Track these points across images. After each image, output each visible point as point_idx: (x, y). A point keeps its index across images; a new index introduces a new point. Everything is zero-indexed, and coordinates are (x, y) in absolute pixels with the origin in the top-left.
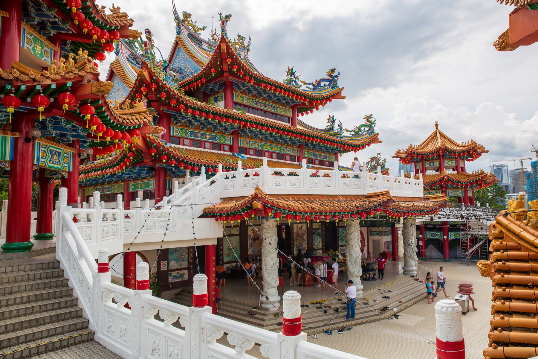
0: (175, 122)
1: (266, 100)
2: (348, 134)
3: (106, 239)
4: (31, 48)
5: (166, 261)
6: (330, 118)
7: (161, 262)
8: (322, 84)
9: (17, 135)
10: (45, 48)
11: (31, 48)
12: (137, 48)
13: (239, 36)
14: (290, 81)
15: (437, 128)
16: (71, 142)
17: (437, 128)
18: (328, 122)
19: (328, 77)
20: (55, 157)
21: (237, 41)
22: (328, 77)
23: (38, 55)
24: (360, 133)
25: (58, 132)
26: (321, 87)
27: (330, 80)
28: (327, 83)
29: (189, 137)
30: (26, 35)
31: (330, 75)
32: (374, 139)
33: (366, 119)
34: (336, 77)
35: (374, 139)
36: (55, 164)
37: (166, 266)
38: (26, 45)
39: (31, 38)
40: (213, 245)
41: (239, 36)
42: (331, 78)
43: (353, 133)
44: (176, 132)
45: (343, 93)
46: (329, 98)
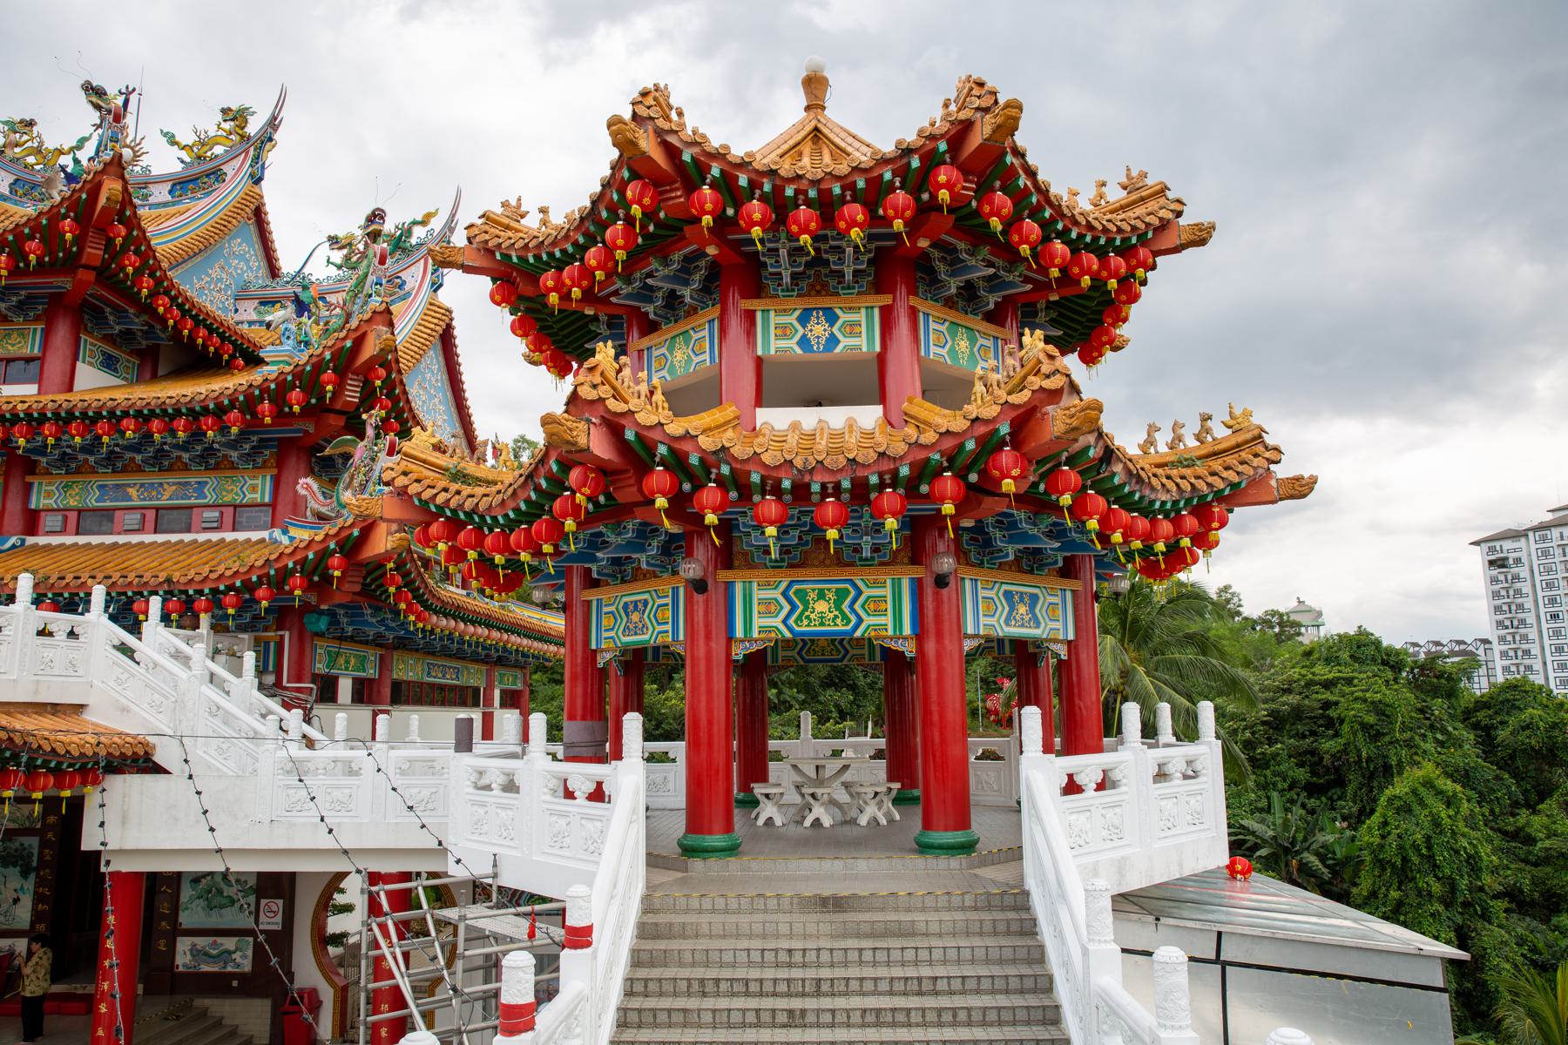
3: (1169, 833)
4: (943, 352)
9: (918, 572)
10: (981, 341)
11: (943, 352)
16: (1060, 564)
20: (1022, 609)
23: (964, 362)
25: (1021, 547)
30: (932, 325)
36: (1022, 626)
38: (933, 349)
39: (943, 328)
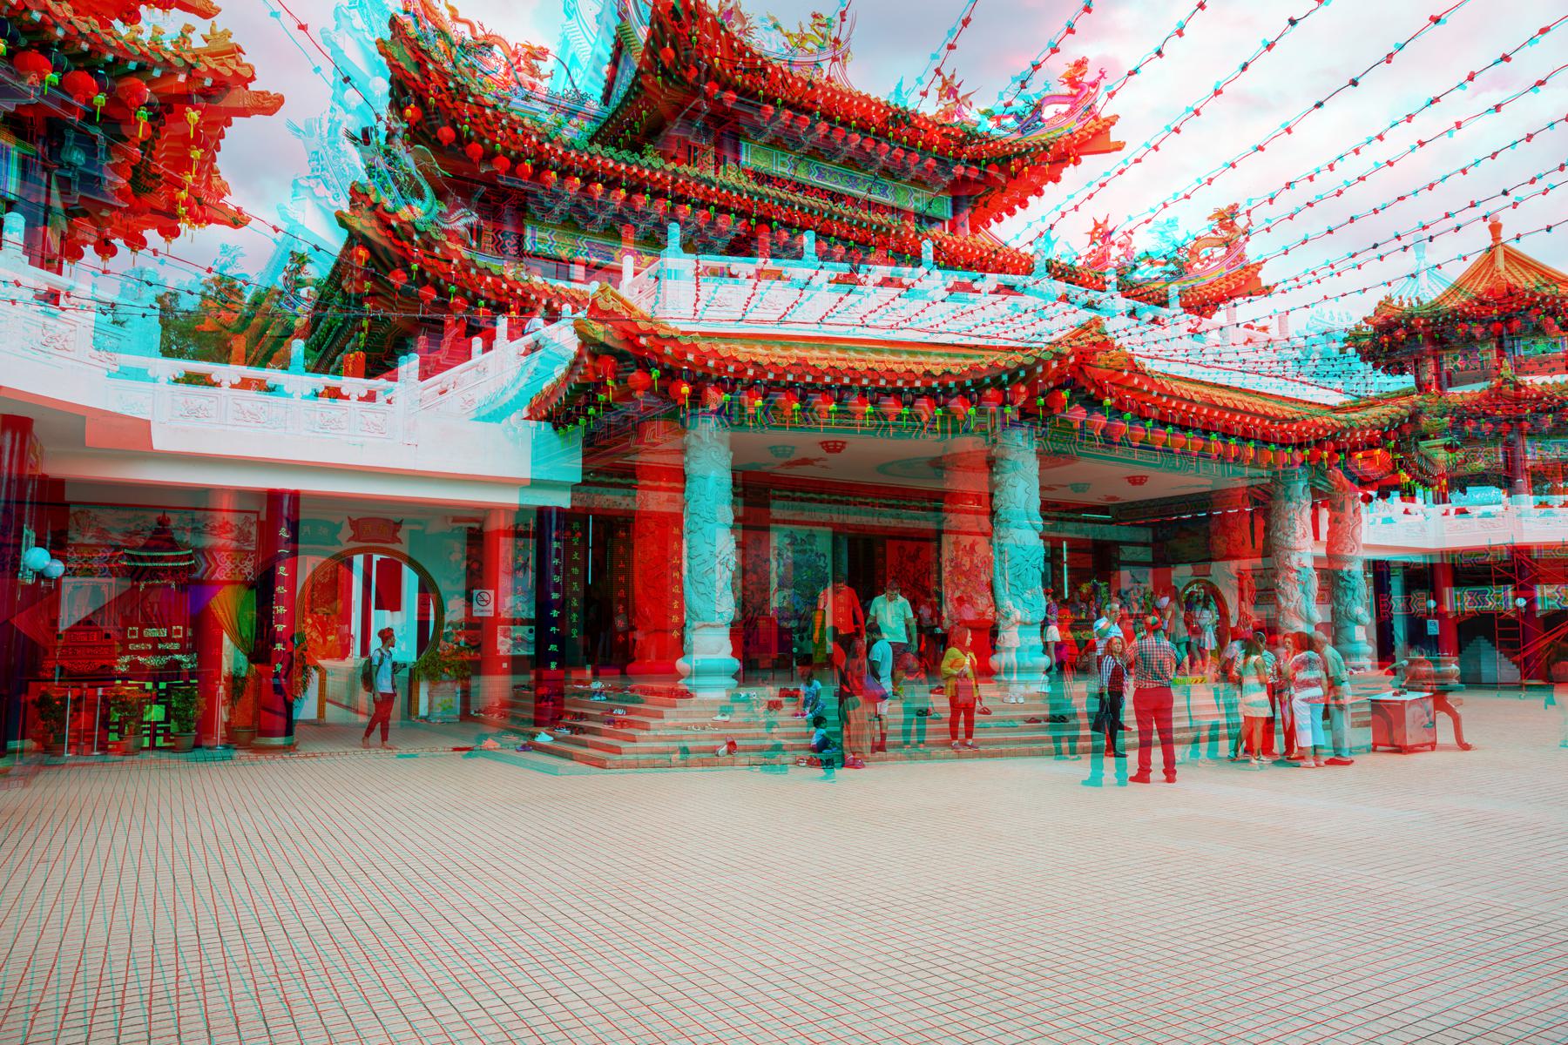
0: (539, 214)
1: (858, 168)
2: (1155, 271)
5: (492, 592)
6: (1097, 226)
7: (476, 592)
8: (1048, 112)
12: (499, 60)
13: (815, 16)
14: (947, 115)
15: (1496, 238)
17: (1496, 238)
18: (1092, 242)
19: (1066, 90)
21: (807, 30)
22: (1066, 90)
24: (1197, 266)
26: (1041, 120)
27: (1071, 96)
28: (1064, 108)
29: (583, 258)
31: (1073, 82)
32: (1246, 284)
33: (1216, 222)
34: (1094, 85)
35: (1246, 284)
37: (491, 606)
40: (559, 509)
41: (815, 16)
42: (1075, 92)
43: (1171, 267)
44: (543, 240)
45: (1115, 134)
46: (1063, 155)
